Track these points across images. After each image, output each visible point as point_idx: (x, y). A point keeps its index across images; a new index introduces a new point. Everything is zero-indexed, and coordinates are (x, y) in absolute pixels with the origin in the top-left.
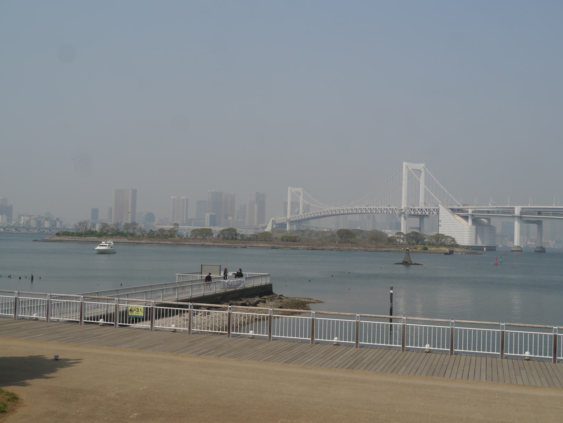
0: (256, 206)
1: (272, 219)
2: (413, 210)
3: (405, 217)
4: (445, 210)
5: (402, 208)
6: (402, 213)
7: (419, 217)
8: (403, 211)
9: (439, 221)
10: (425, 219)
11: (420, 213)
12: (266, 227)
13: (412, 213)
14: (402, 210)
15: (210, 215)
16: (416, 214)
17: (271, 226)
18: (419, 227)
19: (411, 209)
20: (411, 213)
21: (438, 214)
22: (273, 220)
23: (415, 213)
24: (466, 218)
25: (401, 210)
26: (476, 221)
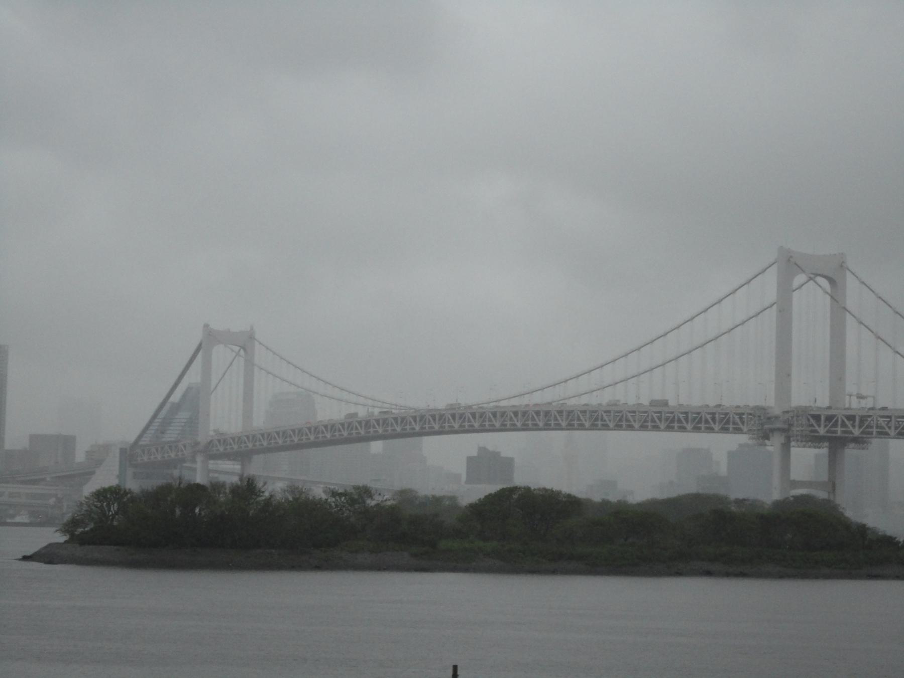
2: (823, 418)
6: (779, 430)
7: (826, 444)
8: (779, 425)
10: (851, 452)
11: (857, 432)
12: (93, 473)
13: (822, 431)
14: (777, 417)
16: (839, 434)
17: (117, 472)
19: (817, 418)
20: (816, 431)
22: (123, 451)
23: (835, 432)
25: (769, 418)
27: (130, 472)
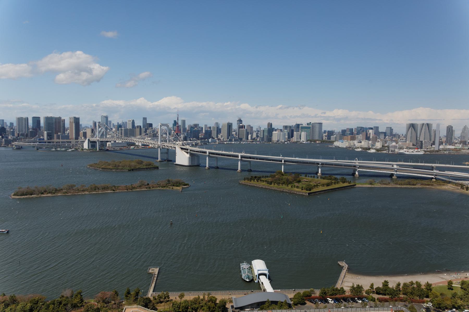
0: (74, 124)
1: (88, 138)
3: (160, 149)
4: (178, 148)
5: (159, 144)
9: (176, 153)
11: (167, 148)
13: (164, 147)
14: (159, 145)
15: (48, 133)
18: (166, 152)
19: (163, 145)
21: (175, 149)
22: (88, 139)
24: (187, 153)
26: (192, 155)
27: (89, 142)
